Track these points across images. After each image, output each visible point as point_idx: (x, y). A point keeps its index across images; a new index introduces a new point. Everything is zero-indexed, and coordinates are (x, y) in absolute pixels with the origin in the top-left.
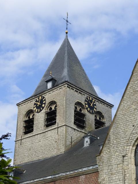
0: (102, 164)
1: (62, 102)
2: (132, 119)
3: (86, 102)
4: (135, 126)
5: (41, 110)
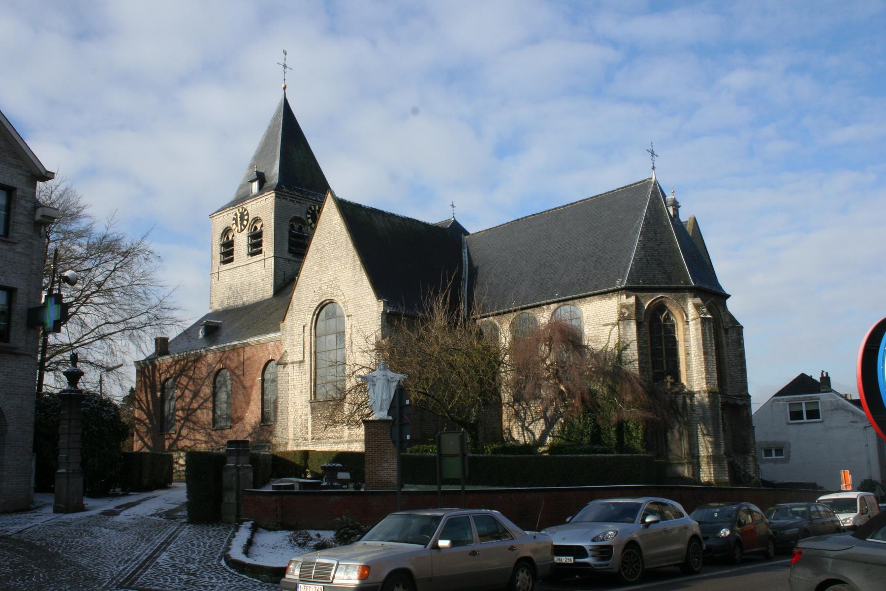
5: (242, 230)
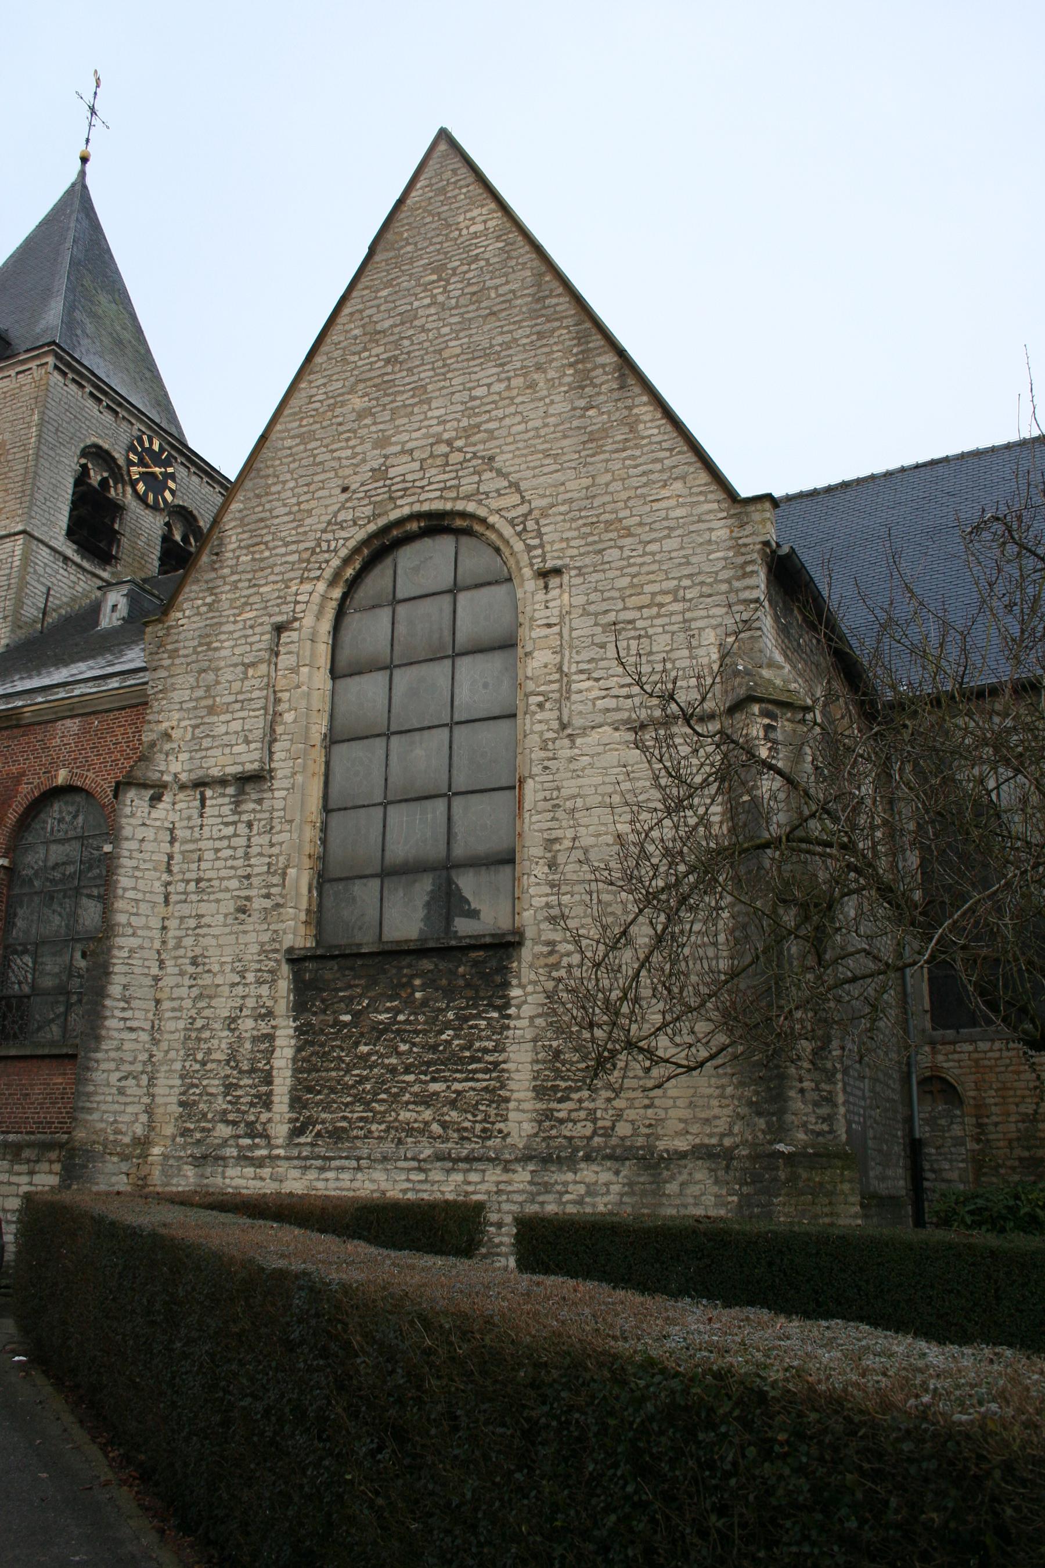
0: (167, 662)
1: (22, 432)
2: (339, 458)
3: (131, 456)
4: (354, 492)
